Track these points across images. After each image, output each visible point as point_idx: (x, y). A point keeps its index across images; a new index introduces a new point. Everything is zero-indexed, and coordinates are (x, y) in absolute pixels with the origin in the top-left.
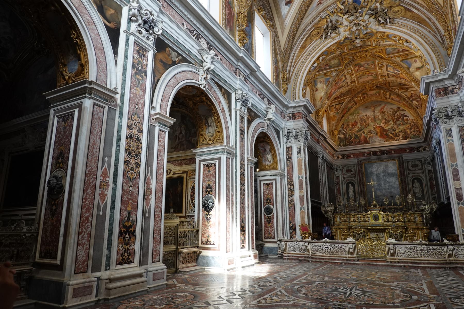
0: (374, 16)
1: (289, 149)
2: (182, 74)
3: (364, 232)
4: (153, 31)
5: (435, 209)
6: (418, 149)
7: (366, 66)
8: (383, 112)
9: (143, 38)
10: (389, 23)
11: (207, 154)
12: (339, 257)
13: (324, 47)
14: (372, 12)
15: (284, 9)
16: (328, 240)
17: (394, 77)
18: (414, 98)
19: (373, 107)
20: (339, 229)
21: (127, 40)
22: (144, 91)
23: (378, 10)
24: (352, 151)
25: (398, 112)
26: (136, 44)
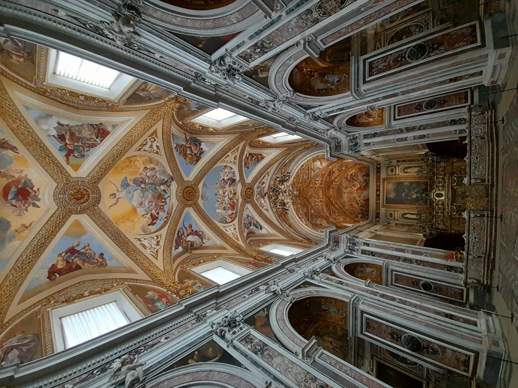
1: (364, 252)
2: (278, 313)
3: (455, 206)
4: (238, 322)
5: (433, 153)
6: (380, 168)
7: (313, 192)
9: (239, 333)
11: (356, 322)
12: (487, 228)
13: (293, 213)
15: (264, 232)
16: (465, 235)
20: (451, 227)
21: (235, 347)
22: (279, 354)
26: (241, 341)
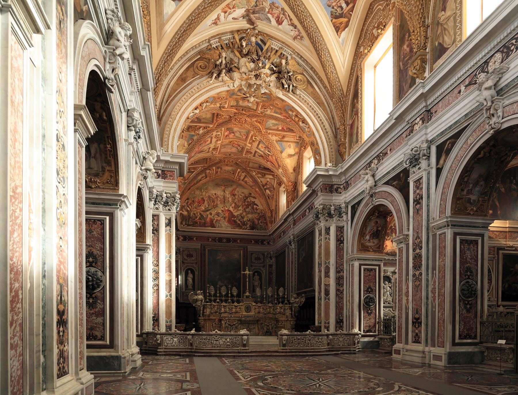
0: (276, 75)
7: (238, 134)
8: (234, 195)
10: (291, 91)
14: (275, 69)
17: (261, 157)
18: (268, 186)
19: (224, 186)
23: (283, 69)
24: (196, 233)
25: (249, 198)
